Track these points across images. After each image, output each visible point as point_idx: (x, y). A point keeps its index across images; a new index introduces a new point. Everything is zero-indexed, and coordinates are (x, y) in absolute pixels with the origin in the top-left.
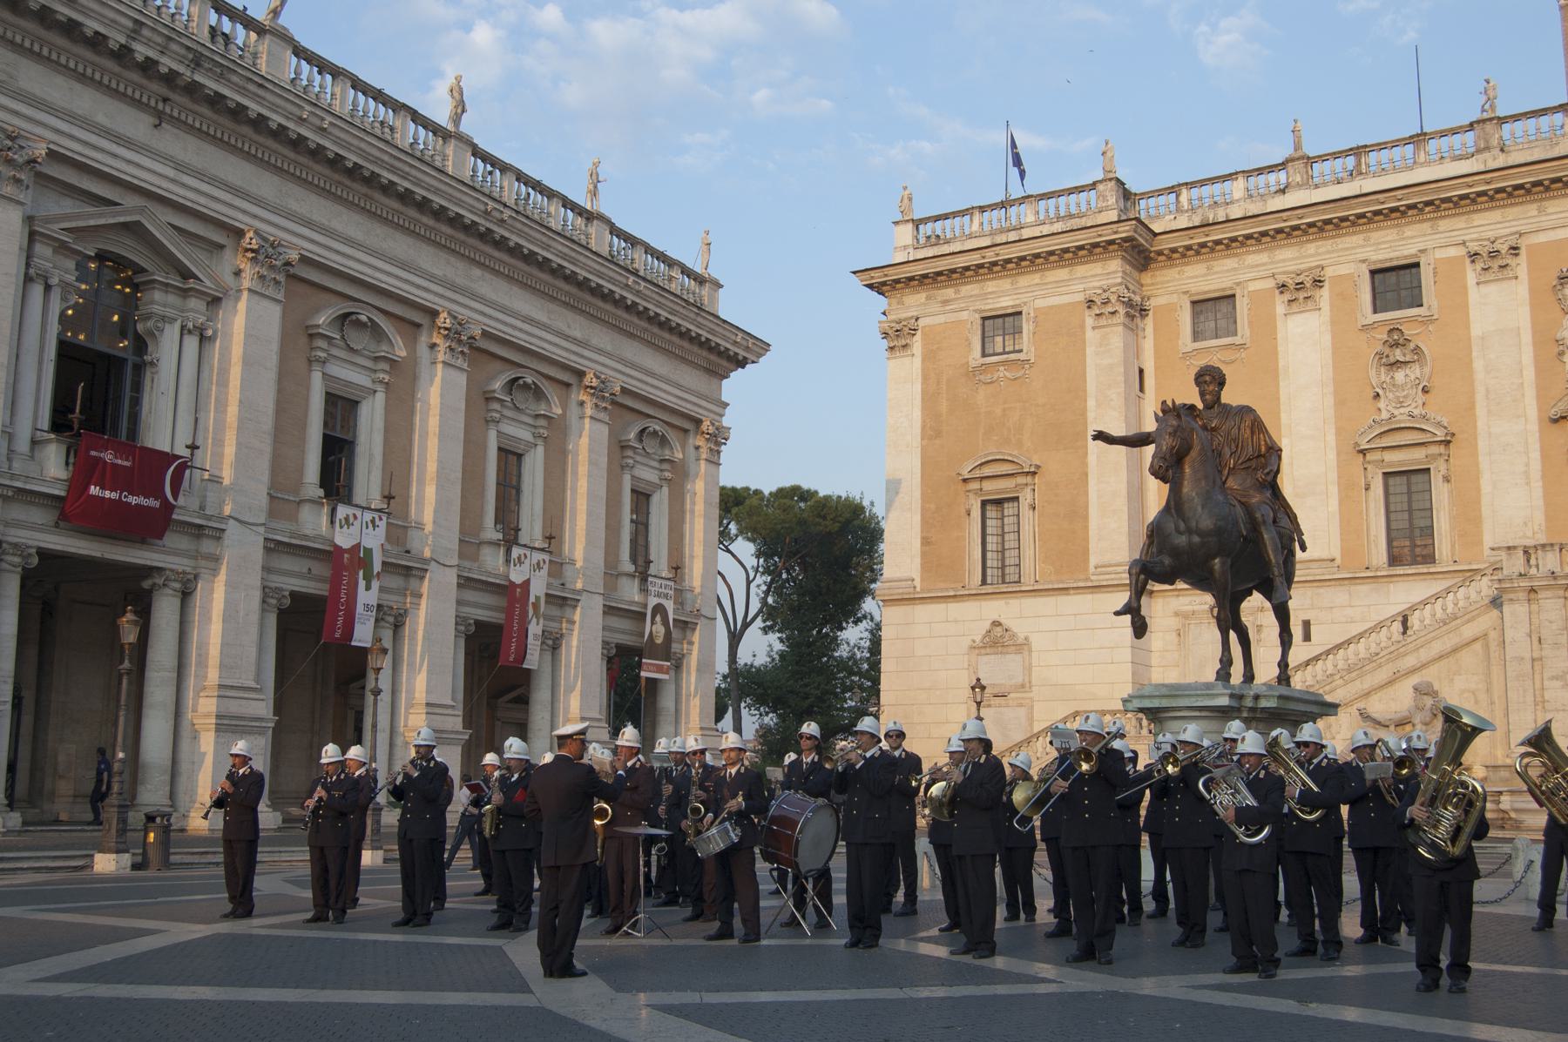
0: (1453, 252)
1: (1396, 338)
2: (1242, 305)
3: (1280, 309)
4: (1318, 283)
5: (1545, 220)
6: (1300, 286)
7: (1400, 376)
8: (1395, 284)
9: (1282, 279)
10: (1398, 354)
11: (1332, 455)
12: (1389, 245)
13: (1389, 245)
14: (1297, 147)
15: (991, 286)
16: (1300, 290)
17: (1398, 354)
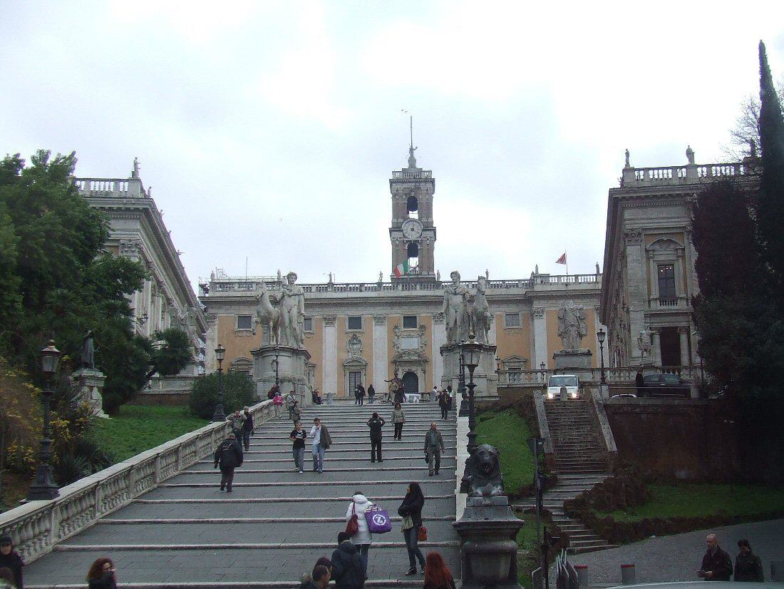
0: (369, 316)
1: (355, 337)
2: (313, 322)
3: (324, 324)
4: (334, 319)
5: (393, 311)
6: (330, 320)
7: (355, 347)
8: (355, 322)
9: (325, 316)
10: (355, 341)
11: (336, 366)
12: (354, 312)
13: (354, 312)
14: (331, 280)
15: (242, 307)
16: (330, 321)
17: (355, 341)
